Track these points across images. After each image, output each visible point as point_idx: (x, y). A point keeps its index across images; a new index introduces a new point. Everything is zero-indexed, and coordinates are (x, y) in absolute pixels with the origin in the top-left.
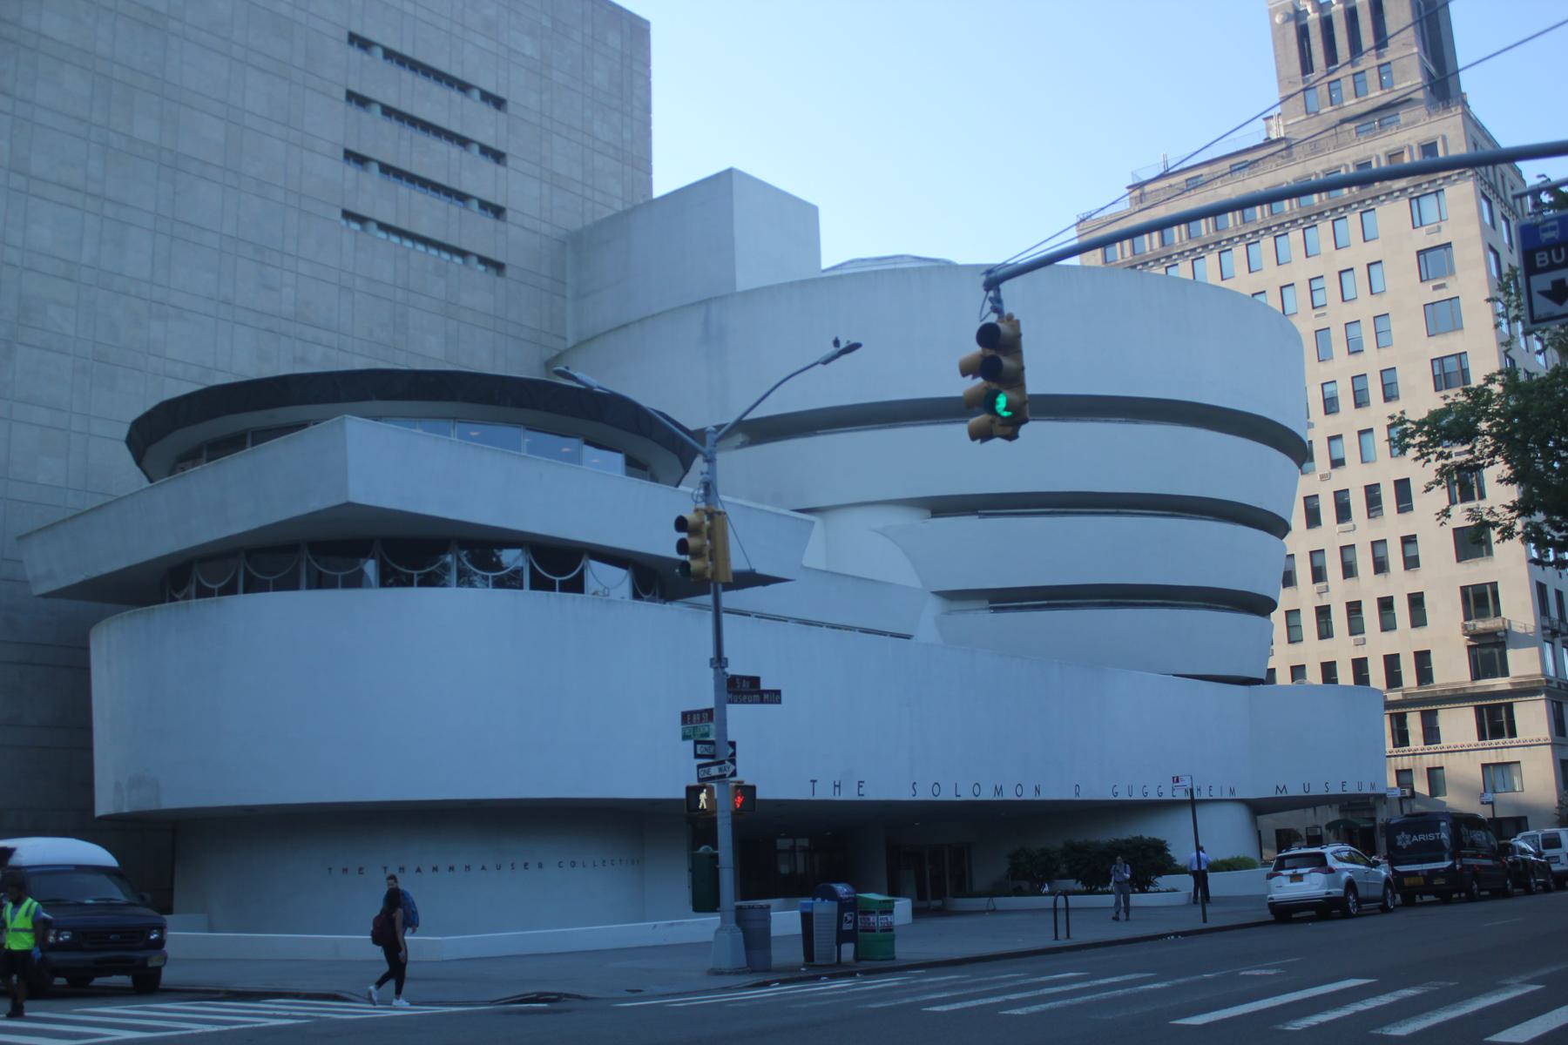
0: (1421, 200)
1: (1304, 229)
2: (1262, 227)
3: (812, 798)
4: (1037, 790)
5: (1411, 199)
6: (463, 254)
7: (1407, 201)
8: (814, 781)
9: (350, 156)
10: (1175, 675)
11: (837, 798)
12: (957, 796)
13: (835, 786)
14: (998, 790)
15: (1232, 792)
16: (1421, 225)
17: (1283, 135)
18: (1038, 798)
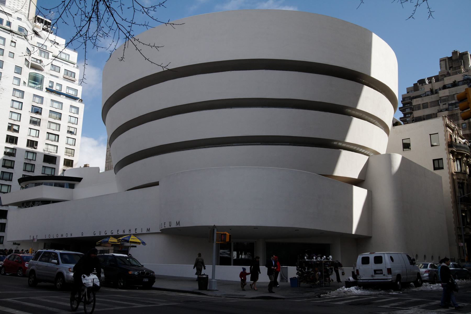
4: (71, 235)
8: (30, 236)
14: (62, 235)
15: (148, 230)
18: (72, 237)
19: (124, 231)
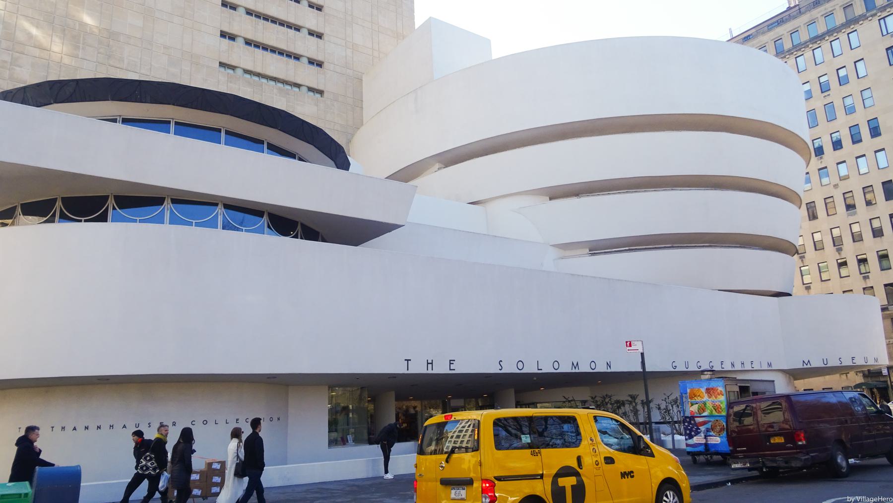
0: (886, 19)
1: (813, 50)
2: (787, 54)
3: (406, 372)
4: (609, 365)
5: (879, 20)
6: (298, 86)
7: (878, 21)
8: (408, 360)
9: (223, 35)
10: (719, 290)
11: (430, 371)
12: (538, 369)
13: (428, 363)
15: (770, 365)
16: (888, 34)
17: (797, 3)
18: (609, 370)
19: (733, 365)
